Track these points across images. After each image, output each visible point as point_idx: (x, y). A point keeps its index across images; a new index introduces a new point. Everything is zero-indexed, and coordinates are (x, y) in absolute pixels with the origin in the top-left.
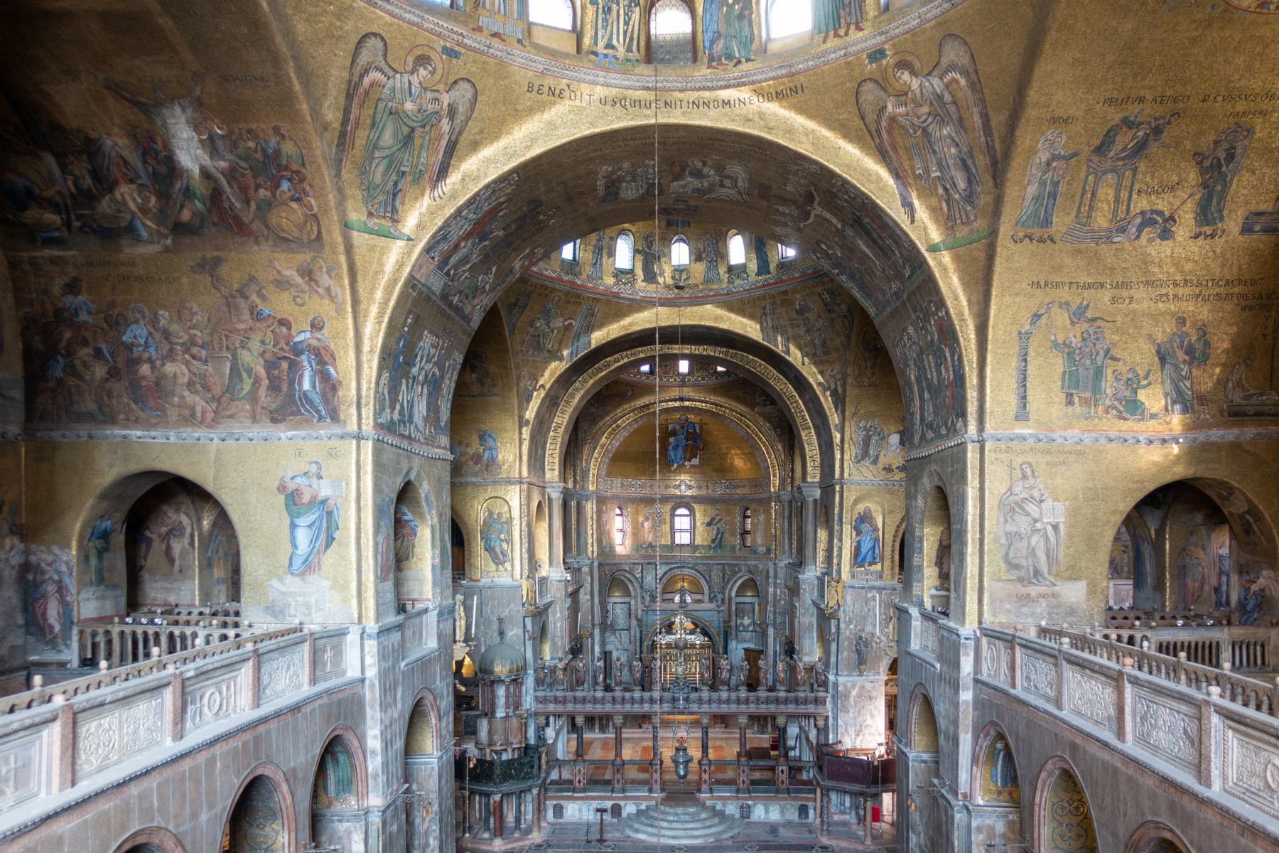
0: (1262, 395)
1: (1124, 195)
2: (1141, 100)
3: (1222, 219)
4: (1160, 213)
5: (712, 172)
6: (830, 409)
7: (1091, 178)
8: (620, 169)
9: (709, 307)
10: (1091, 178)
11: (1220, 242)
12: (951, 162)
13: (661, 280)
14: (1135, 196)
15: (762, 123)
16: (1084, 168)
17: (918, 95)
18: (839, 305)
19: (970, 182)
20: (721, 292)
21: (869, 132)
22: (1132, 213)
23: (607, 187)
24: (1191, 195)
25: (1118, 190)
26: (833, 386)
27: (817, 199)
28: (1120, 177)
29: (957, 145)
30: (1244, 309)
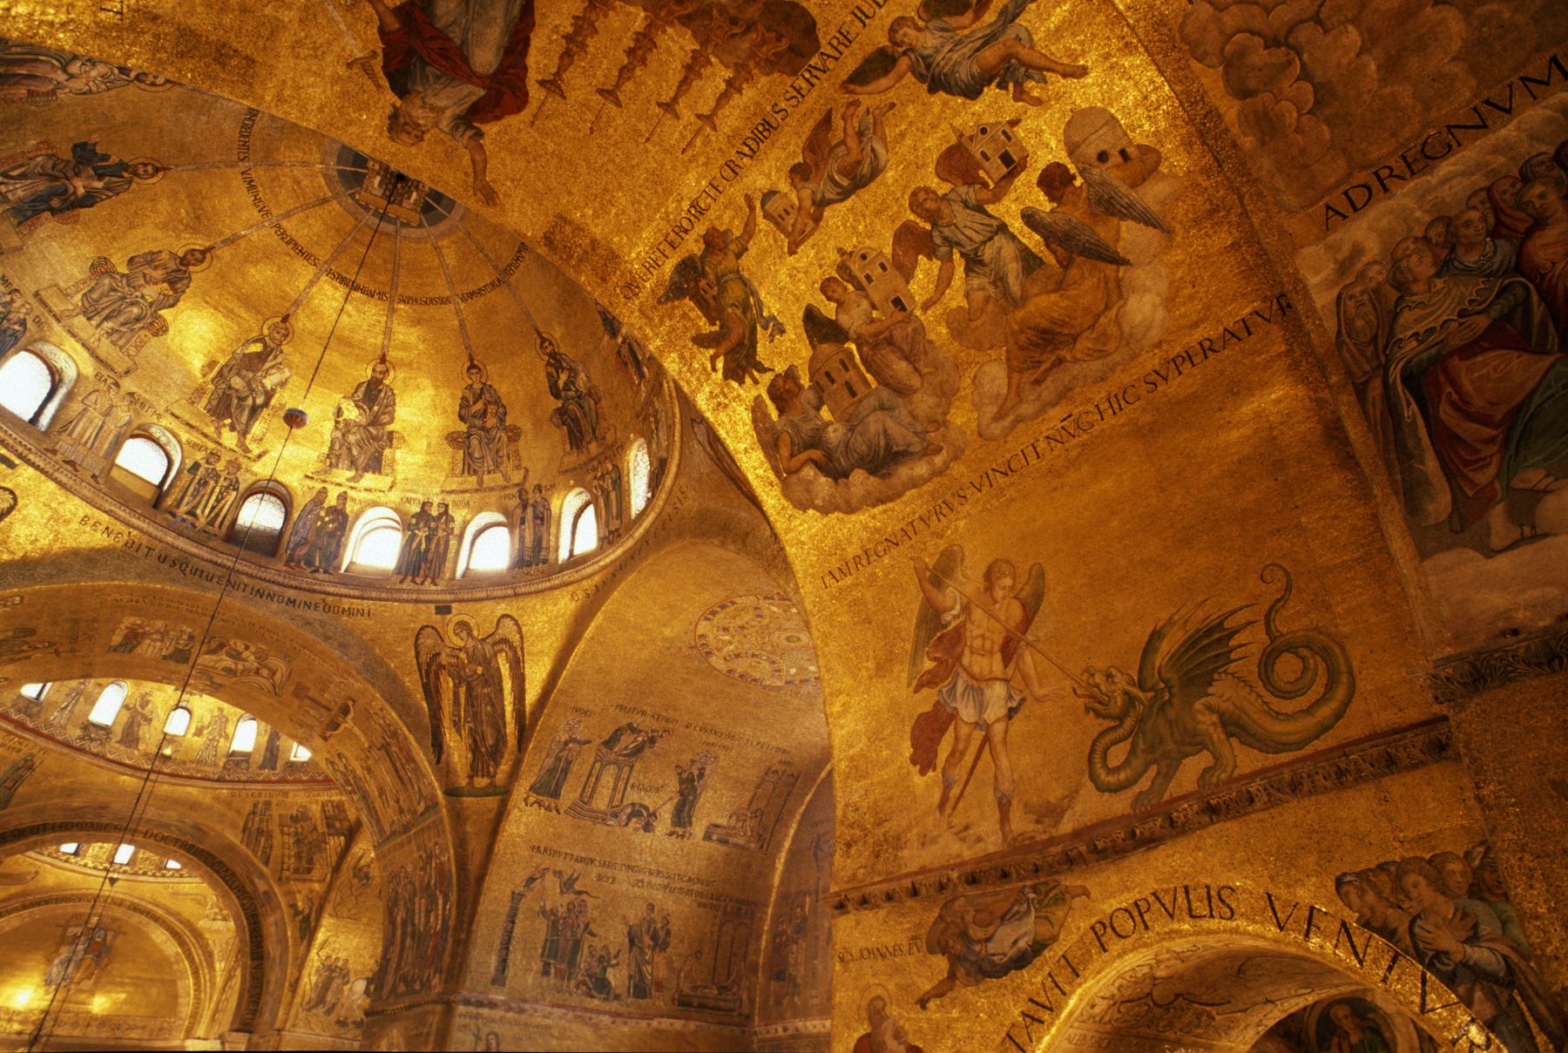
0: (706, 987)
1: (621, 785)
2: (644, 713)
3: (690, 824)
4: (646, 808)
5: (252, 658)
6: (295, 940)
7: (598, 765)
8: (149, 625)
9: (189, 789)
10: (598, 765)
11: (687, 843)
12: (484, 718)
13: (142, 747)
14: (629, 789)
15: (320, 630)
16: (594, 755)
17: (471, 650)
18: (341, 821)
19: (497, 740)
20: (212, 776)
21: (420, 671)
22: (625, 803)
23: (126, 637)
24: (671, 799)
25: (617, 780)
26: (306, 911)
27: (351, 715)
28: (620, 770)
29: (493, 706)
30: (700, 905)
